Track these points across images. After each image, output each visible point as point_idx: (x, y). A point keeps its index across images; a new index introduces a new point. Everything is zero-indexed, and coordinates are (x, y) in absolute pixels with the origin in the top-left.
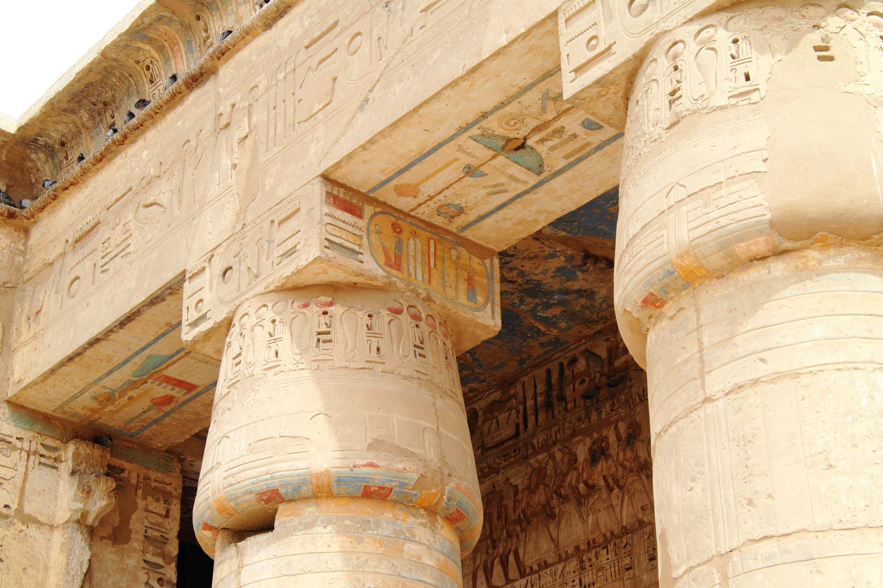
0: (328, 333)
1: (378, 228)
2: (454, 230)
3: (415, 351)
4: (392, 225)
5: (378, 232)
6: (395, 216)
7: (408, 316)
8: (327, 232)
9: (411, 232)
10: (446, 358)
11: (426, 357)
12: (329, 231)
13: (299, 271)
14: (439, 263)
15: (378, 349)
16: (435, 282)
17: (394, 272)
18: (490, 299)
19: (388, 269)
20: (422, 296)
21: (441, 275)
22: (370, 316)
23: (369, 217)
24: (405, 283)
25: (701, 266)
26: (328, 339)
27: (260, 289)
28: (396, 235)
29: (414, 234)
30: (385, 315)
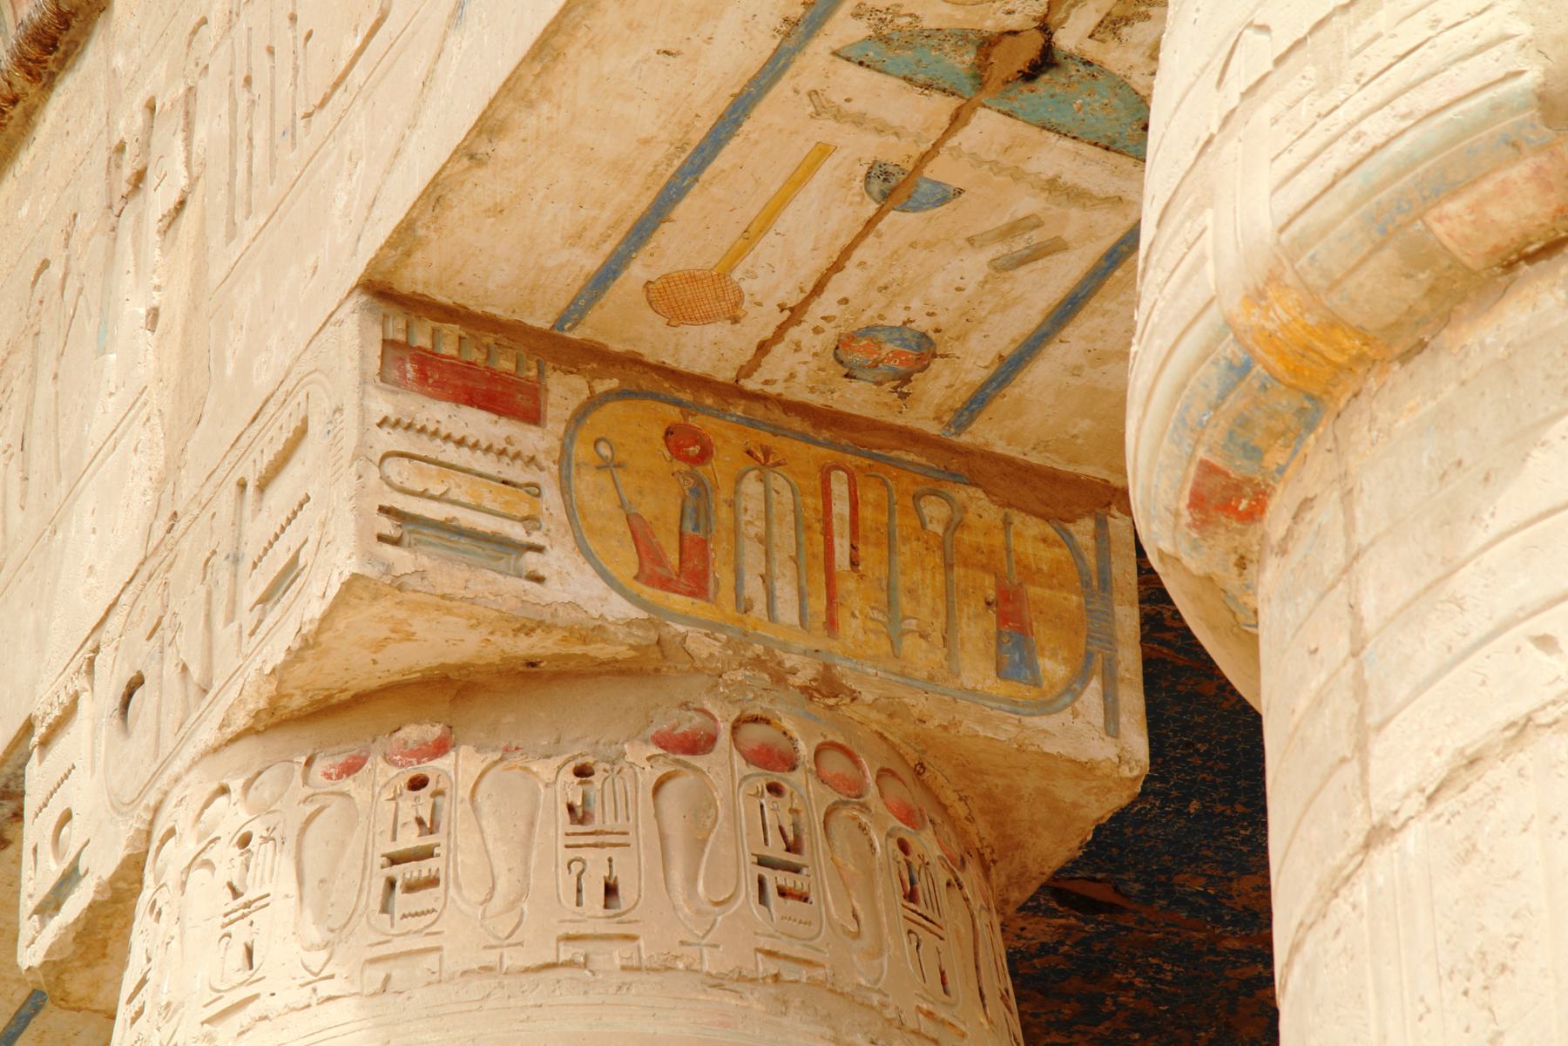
0: (426, 854)
1: (605, 450)
2: (933, 429)
3: (761, 882)
4: (668, 433)
5: (605, 466)
6: (678, 403)
7: (736, 756)
8: (390, 484)
9: (749, 452)
10: (911, 896)
11: (812, 898)
12: (396, 479)
13: (308, 645)
14: (866, 552)
15: (611, 890)
16: (856, 623)
17: (679, 602)
18: (1098, 666)
19: (650, 593)
20: (799, 680)
21: (883, 597)
22: (583, 772)
23: (568, 414)
24: (723, 637)
25: (1333, 323)
26: (425, 874)
27: (208, 734)
28: (684, 467)
29: (764, 460)
30: (644, 765)
